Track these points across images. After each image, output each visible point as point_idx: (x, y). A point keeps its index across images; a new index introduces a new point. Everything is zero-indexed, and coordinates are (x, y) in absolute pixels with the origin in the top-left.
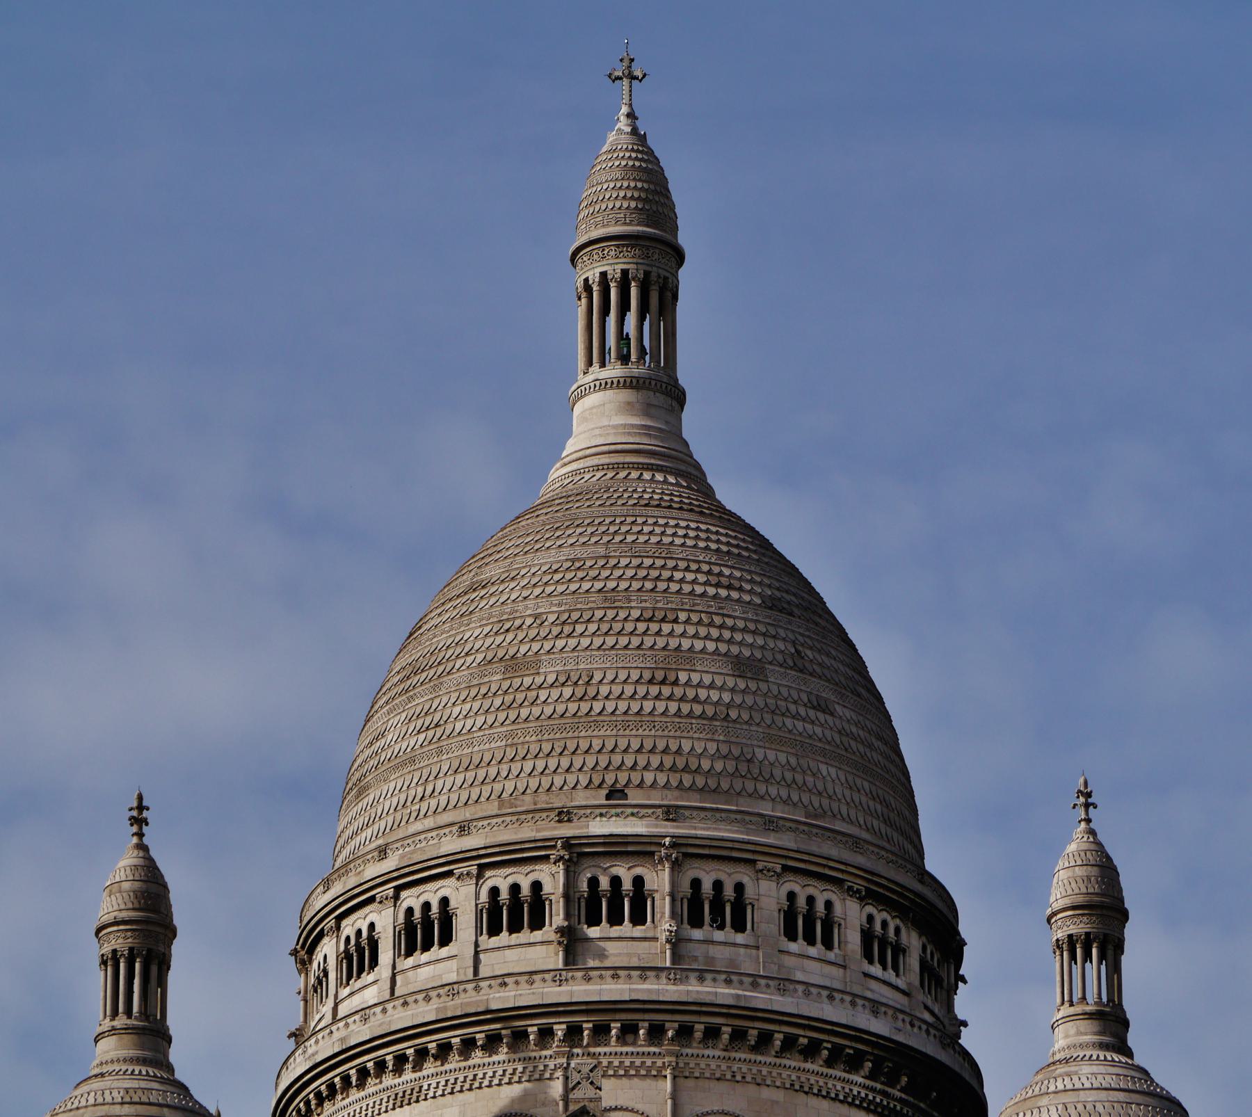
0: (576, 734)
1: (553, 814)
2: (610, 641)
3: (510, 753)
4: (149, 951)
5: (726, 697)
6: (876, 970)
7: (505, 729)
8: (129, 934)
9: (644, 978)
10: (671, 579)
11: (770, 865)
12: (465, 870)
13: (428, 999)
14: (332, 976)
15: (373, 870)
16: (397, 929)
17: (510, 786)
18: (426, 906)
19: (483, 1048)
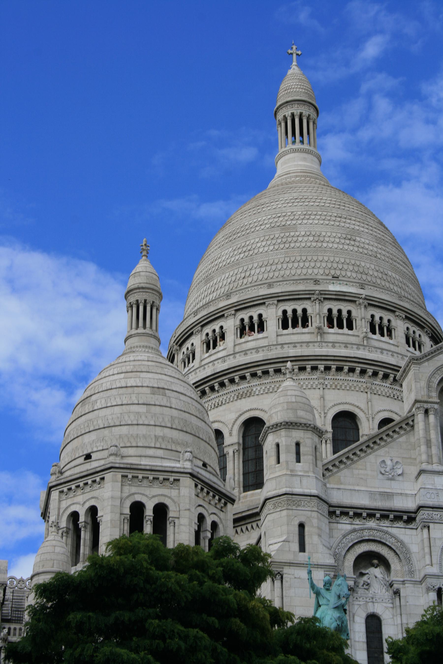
0: (316, 254)
1: (312, 281)
3: (287, 259)
4: (153, 302)
5: (375, 249)
7: (284, 251)
8: (144, 293)
9: (358, 349)
11: (401, 314)
12: (271, 302)
13: (257, 352)
15: (222, 304)
16: (236, 328)
17: (288, 272)
18: (251, 318)
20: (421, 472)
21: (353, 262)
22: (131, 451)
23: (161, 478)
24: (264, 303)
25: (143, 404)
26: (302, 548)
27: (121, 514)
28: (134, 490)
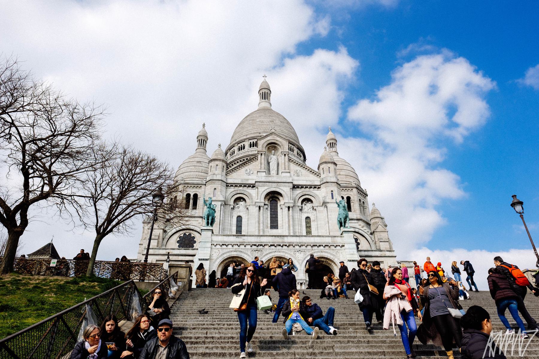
6: (298, 157)
17: (252, 132)
18: (241, 145)
20: (258, 172)
22: (188, 179)
23: (196, 186)
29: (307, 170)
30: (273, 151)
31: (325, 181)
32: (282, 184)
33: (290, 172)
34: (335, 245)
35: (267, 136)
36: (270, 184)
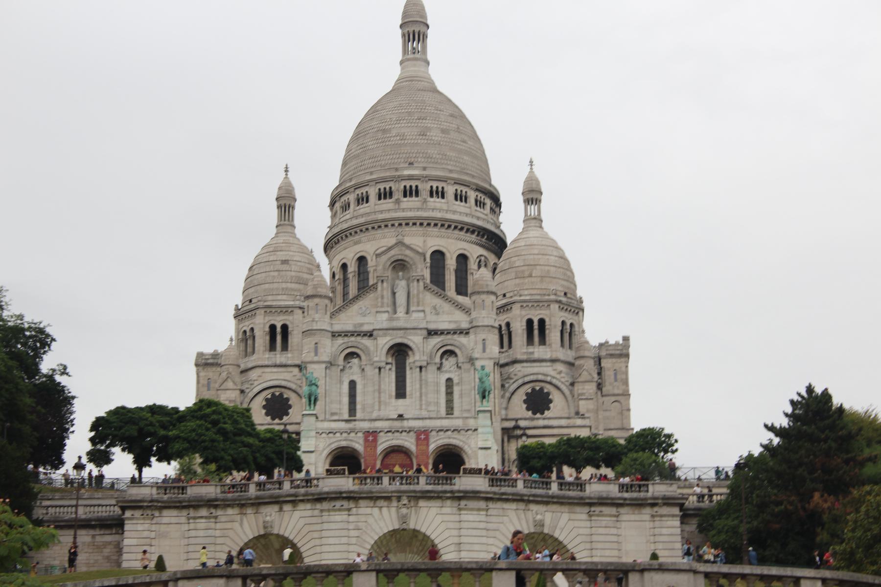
2: (409, 125)
4: (289, 205)
5: (440, 139)
6: (478, 209)
9: (418, 211)
10: (425, 109)
13: (362, 217)
14: (338, 212)
15: (348, 185)
17: (383, 163)
18: (362, 193)
19: (376, 229)
21: (423, 151)
22: (270, 298)
23: (284, 311)
24: (368, 185)
25: (276, 271)
26: (316, 354)
27: (264, 331)
28: (270, 318)
29: (451, 303)
30: (401, 274)
31: (474, 324)
32: (412, 331)
33: (423, 311)
34: (466, 429)
35: (390, 249)
36: (395, 332)
